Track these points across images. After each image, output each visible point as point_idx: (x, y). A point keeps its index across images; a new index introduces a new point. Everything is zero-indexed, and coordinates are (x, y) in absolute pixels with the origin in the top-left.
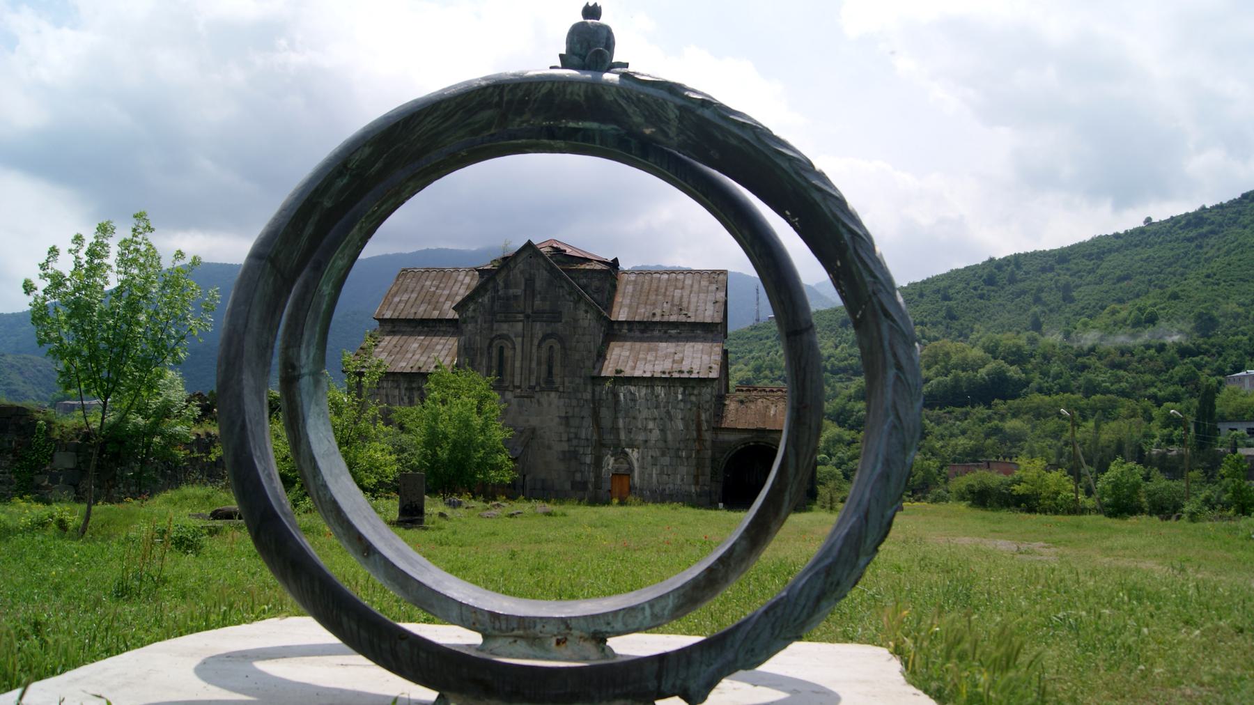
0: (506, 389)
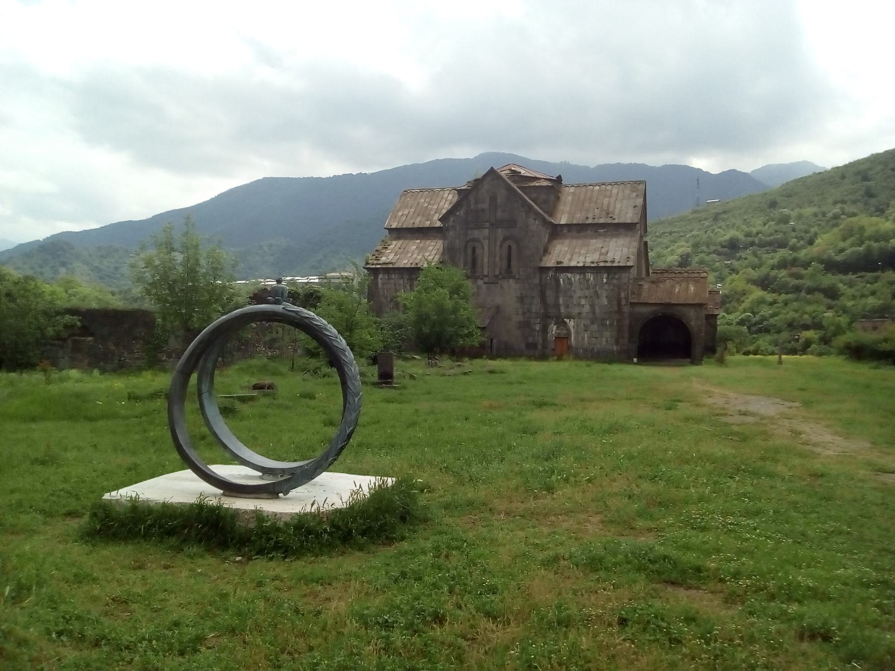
0: (477, 278)
